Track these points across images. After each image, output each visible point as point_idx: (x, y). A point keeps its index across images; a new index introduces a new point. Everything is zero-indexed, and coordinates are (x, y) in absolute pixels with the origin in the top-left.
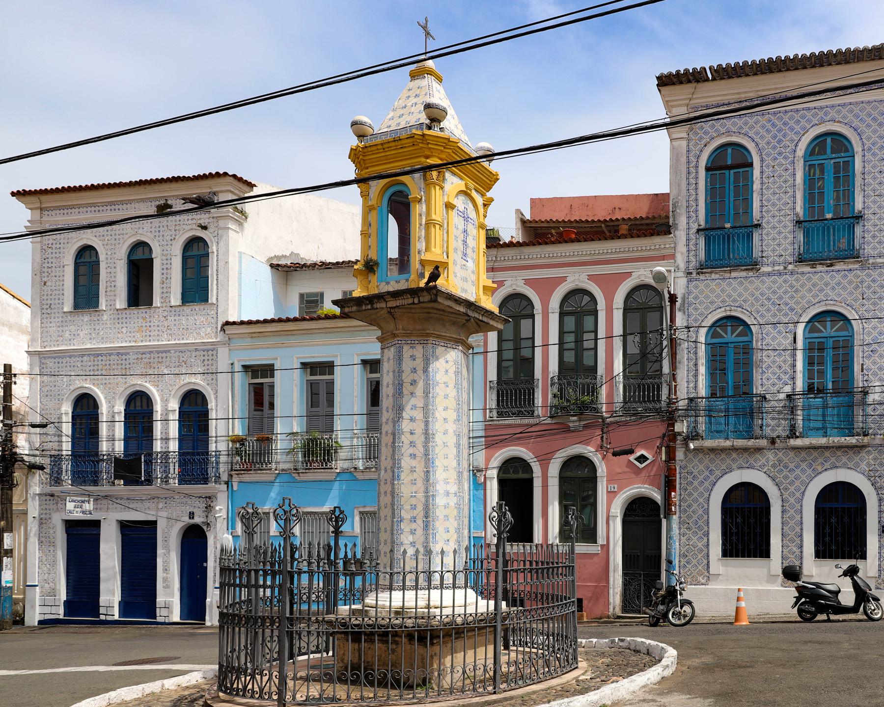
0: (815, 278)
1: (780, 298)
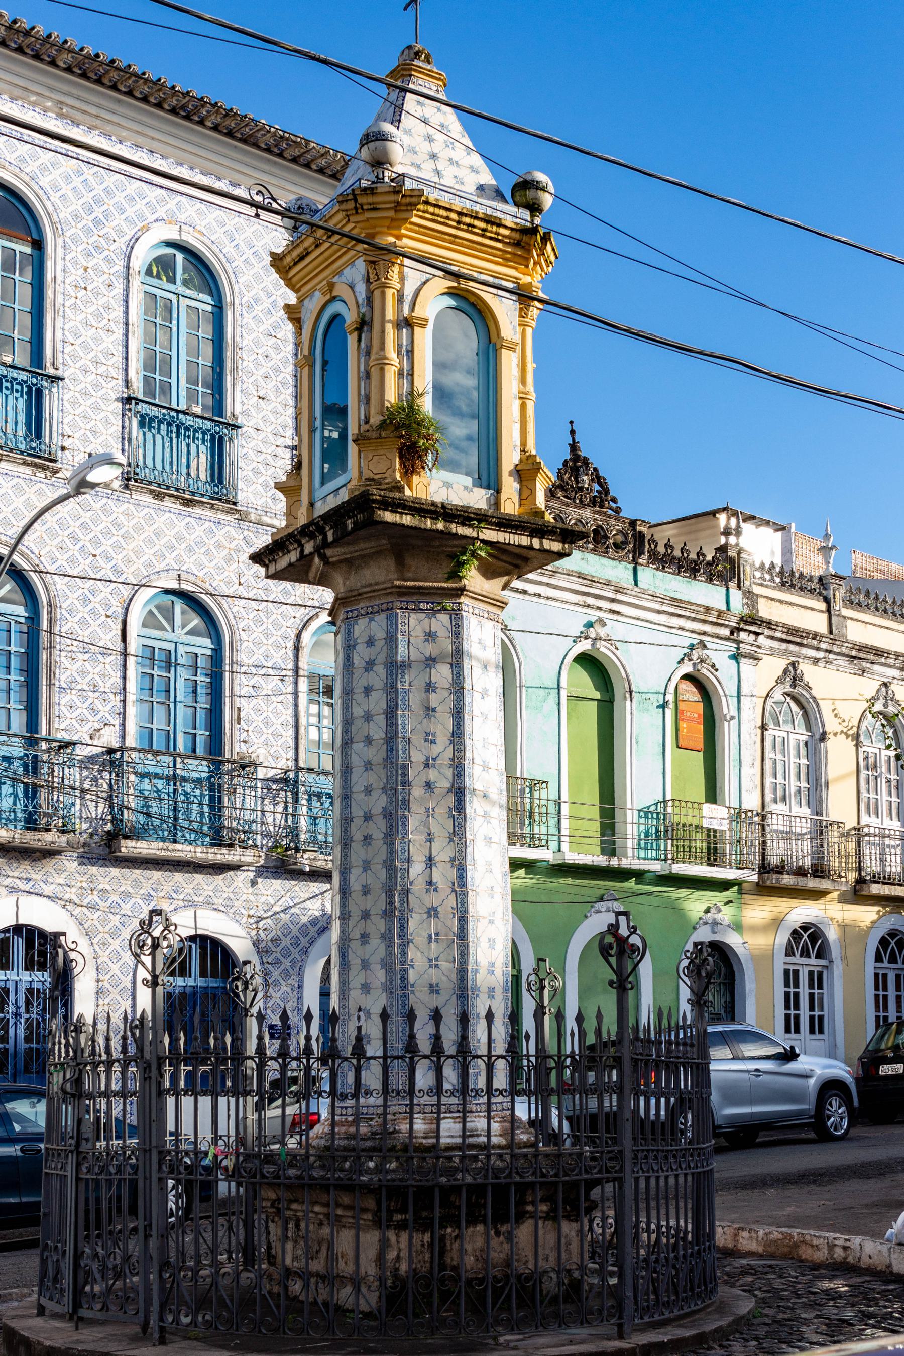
0: (162, 520)
1: (96, 542)
